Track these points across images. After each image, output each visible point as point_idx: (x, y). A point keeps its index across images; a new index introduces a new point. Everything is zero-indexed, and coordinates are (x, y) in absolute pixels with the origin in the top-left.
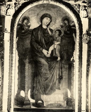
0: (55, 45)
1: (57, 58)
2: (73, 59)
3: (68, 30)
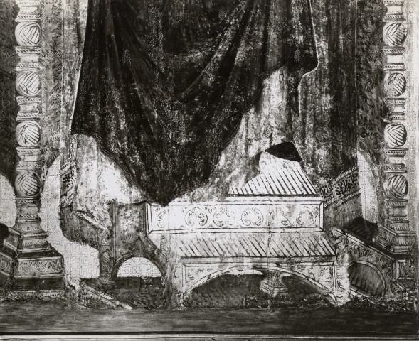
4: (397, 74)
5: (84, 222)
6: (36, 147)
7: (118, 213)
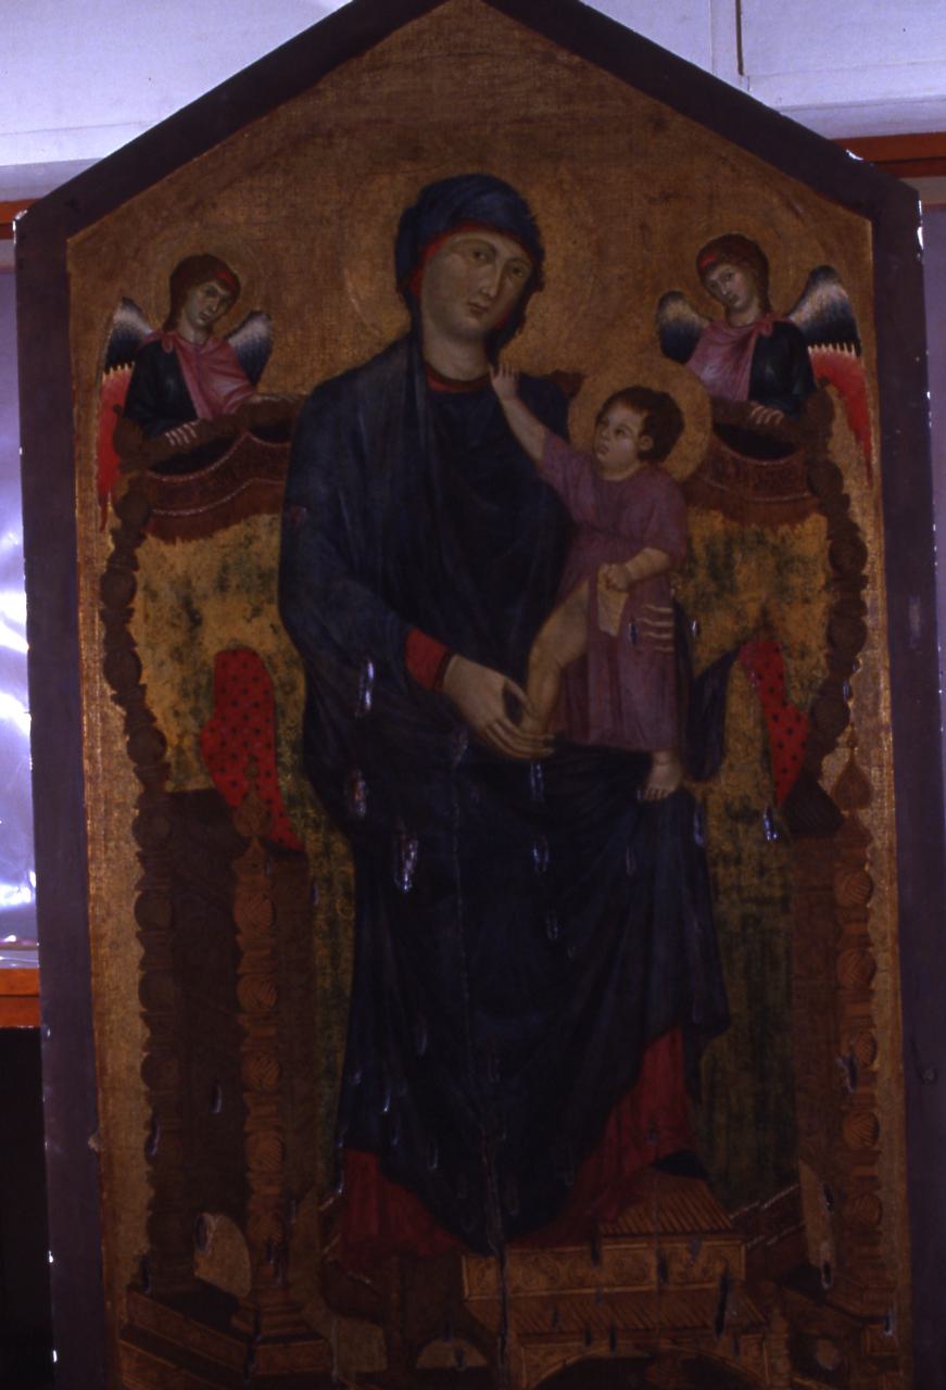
1: (643, 763)
2: (852, 773)
3: (759, 391)
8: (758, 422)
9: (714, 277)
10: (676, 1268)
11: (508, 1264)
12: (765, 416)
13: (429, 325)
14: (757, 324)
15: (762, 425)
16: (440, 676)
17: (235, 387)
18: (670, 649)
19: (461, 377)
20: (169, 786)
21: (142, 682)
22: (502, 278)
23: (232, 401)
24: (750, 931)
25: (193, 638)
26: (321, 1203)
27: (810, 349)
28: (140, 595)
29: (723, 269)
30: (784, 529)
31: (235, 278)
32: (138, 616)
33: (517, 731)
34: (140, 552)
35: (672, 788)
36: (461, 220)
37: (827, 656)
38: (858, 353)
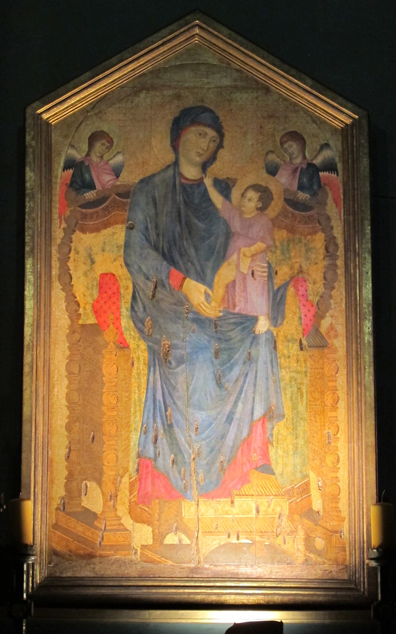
0: (244, 255)
3: (301, 188)
4: (333, 423)
5: (144, 511)
6: (114, 466)
7: (164, 505)
8: (301, 198)
9: (286, 146)
10: (262, 509)
11: (200, 506)
12: (303, 197)
13: (182, 160)
14: (301, 163)
15: (302, 200)
16: (181, 286)
17: (110, 179)
18: (266, 279)
19: (193, 178)
20: (81, 322)
21: (72, 284)
22: (209, 143)
23: (109, 183)
24: (293, 383)
25: (91, 269)
26: (130, 479)
27: (320, 173)
28: (73, 252)
29: (290, 143)
30: (309, 237)
31: (112, 139)
32: (71, 259)
33: (209, 306)
34: (74, 237)
35: (265, 330)
36: (194, 123)
37: (324, 284)
38: (338, 175)
